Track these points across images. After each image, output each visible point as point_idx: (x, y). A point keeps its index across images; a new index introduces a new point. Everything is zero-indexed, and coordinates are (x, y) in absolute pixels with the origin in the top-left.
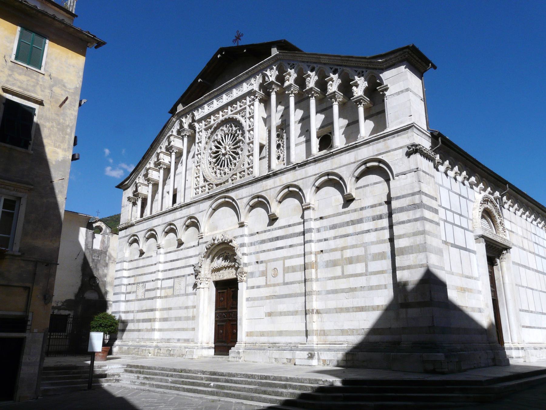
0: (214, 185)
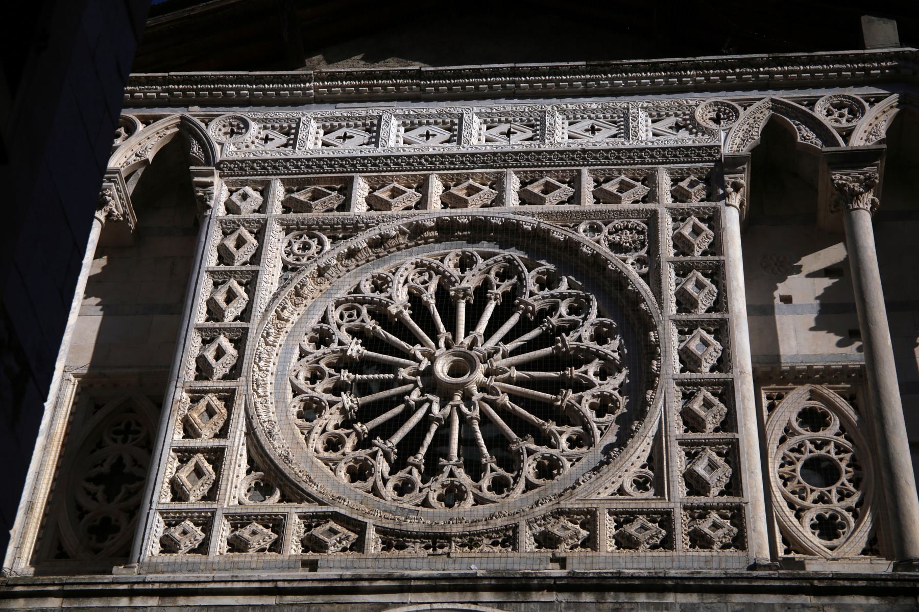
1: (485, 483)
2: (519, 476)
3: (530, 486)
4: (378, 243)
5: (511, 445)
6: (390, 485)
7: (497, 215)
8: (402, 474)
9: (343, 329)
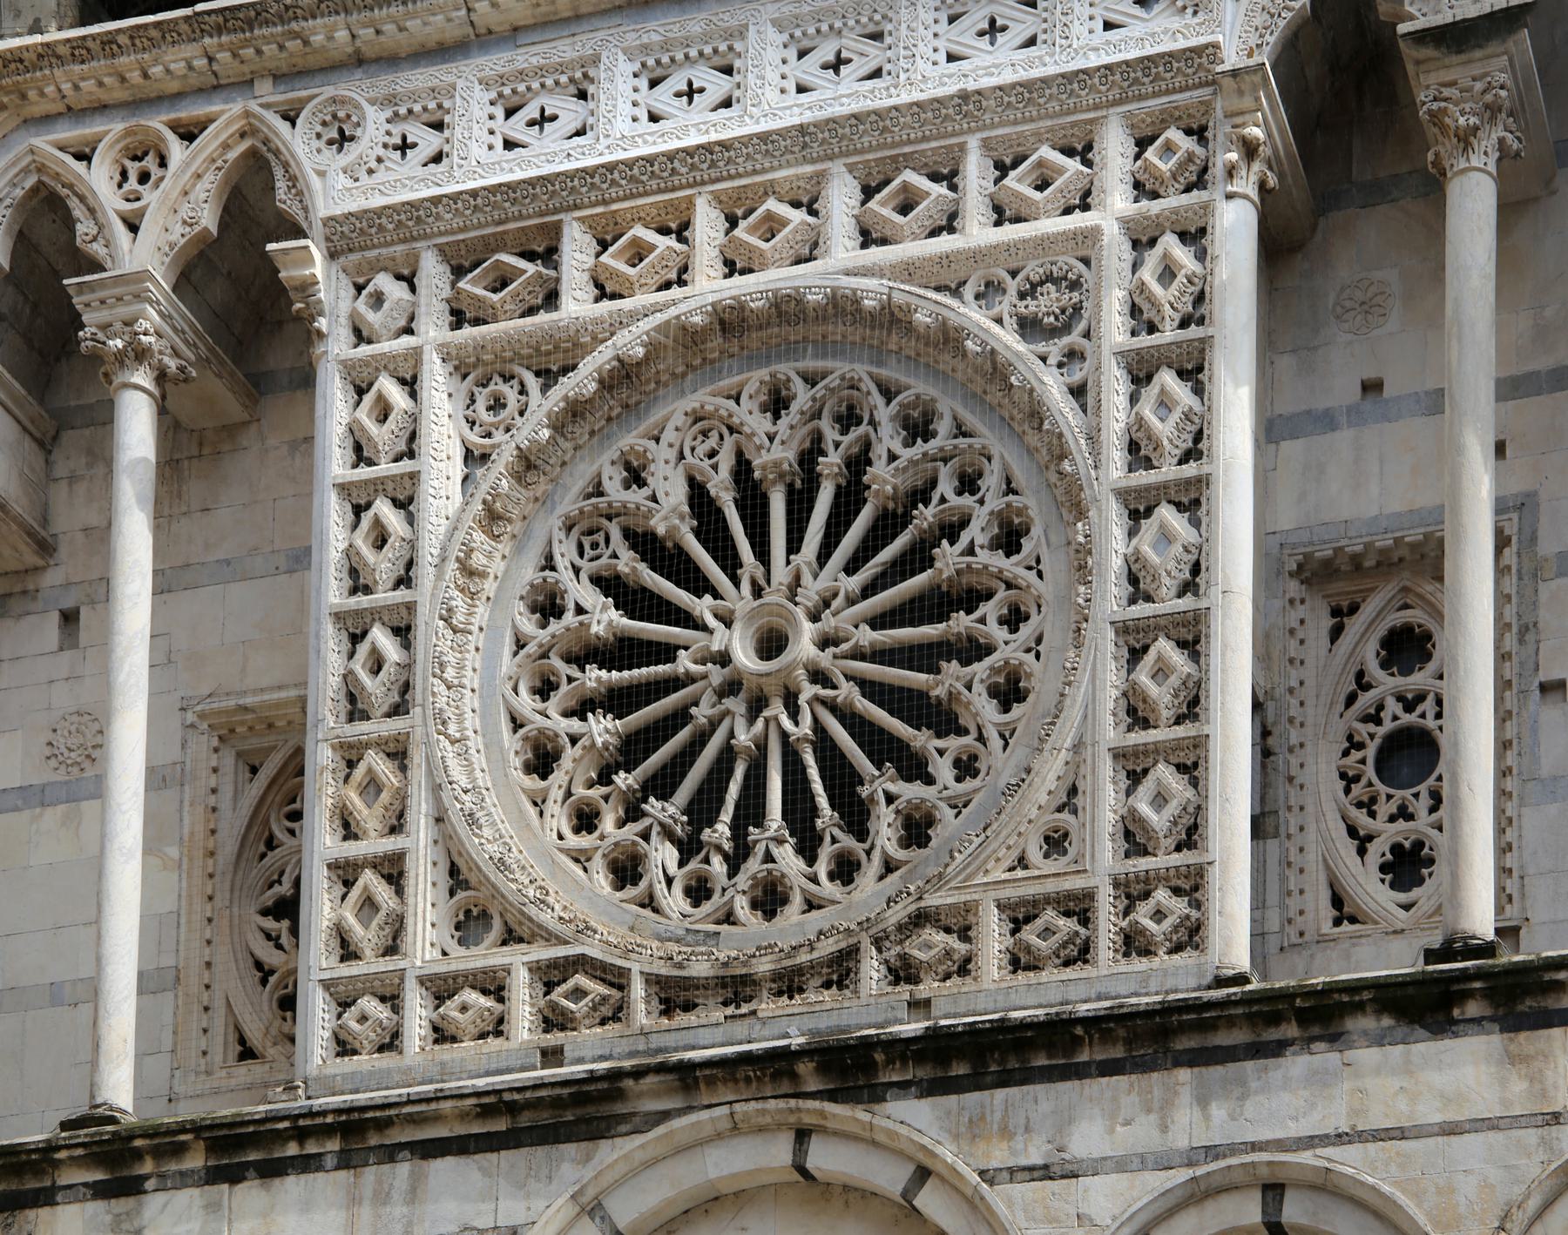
0: (638, 989)
1: (822, 868)
2: (872, 847)
3: (889, 867)
4: (623, 376)
5: (859, 789)
6: (678, 888)
7: (819, 283)
8: (694, 865)
9: (584, 576)
